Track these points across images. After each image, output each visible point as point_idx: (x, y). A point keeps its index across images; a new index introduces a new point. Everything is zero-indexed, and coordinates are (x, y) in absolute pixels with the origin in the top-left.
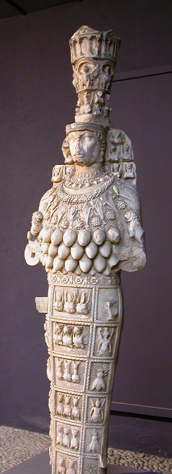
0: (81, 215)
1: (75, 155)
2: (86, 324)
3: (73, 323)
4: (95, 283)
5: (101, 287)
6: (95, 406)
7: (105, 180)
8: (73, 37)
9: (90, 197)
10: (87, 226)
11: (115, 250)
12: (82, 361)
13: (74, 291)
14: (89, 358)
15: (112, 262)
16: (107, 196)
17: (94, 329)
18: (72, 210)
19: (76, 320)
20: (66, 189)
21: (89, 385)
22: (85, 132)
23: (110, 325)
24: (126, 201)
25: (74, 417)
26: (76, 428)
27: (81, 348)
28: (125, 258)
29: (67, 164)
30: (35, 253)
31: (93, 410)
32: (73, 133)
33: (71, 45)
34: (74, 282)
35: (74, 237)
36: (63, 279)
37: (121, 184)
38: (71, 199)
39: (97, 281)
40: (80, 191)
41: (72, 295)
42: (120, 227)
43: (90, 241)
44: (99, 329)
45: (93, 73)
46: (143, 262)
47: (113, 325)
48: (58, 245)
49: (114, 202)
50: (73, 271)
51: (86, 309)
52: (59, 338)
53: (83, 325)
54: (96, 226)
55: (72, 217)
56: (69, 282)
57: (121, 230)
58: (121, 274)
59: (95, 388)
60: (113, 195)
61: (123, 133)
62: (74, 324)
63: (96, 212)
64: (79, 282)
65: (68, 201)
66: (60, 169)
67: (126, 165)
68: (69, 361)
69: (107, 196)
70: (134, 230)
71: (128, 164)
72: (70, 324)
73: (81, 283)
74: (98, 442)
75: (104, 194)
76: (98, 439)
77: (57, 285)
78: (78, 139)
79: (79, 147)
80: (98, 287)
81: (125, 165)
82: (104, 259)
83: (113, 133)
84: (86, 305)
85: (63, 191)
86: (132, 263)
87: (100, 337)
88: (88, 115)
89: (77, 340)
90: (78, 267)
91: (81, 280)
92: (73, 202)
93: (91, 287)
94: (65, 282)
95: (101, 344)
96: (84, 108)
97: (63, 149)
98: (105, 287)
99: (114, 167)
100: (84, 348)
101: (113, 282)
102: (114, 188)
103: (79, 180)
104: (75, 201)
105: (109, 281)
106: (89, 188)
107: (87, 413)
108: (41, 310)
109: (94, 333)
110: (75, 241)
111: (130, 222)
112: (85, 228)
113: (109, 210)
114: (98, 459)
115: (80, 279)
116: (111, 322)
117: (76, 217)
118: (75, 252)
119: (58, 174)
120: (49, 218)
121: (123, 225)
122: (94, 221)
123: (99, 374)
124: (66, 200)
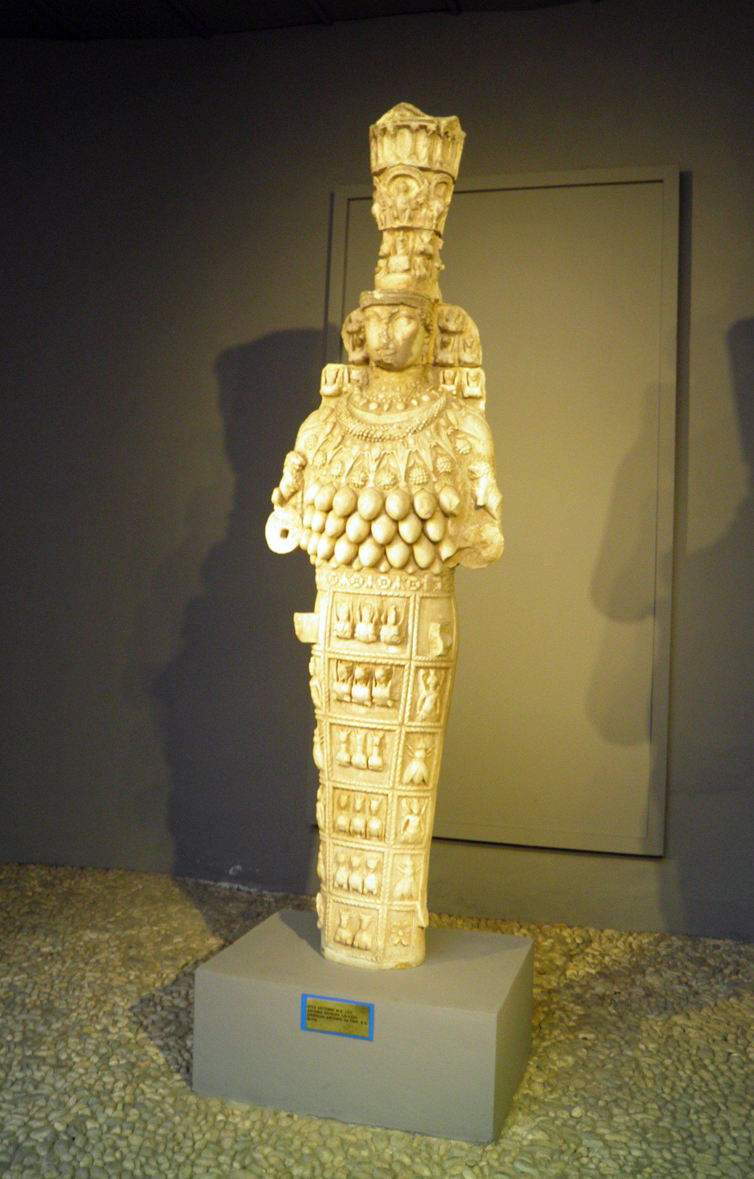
0: (392, 464)
1: (377, 350)
2: (397, 662)
3: (373, 660)
4: (414, 588)
5: (425, 595)
6: (411, 812)
7: (434, 399)
9: (407, 431)
10: (402, 484)
11: (451, 530)
12: (389, 731)
13: (375, 603)
14: (402, 724)
15: (446, 551)
16: (437, 428)
17: (412, 673)
18: (376, 451)
19: (380, 655)
20: (359, 412)
21: (402, 775)
22: (401, 307)
23: (438, 665)
24: (470, 439)
25: (371, 836)
26: (375, 855)
27: (388, 707)
28: (468, 544)
29: (353, 363)
30: (281, 532)
31: (408, 821)
32: (378, 309)
33: (375, 137)
34: (374, 586)
35: (381, 502)
36: (352, 580)
37: (461, 407)
38: (372, 432)
39: (418, 584)
40: (385, 418)
41: (372, 609)
42: (460, 488)
43: (410, 509)
44: (422, 672)
45: (416, 197)
46: (499, 552)
47: (444, 665)
48: (347, 517)
49: (451, 441)
50: (375, 566)
51: (399, 635)
52: (345, 688)
53: (392, 665)
54: (419, 484)
55: (373, 466)
57: (462, 492)
58: (457, 574)
59: (412, 781)
60: (447, 428)
61: (464, 312)
62: (375, 664)
63: (420, 457)
64: (386, 587)
65: (365, 435)
66: (337, 373)
67: (468, 374)
68: (362, 733)
69: (437, 428)
70: (486, 494)
71: (473, 372)
72: (368, 663)
73: (388, 588)
74: (415, 879)
75: (432, 427)
76: (414, 874)
77: (339, 590)
78: (386, 321)
80: (419, 594)
81: (465, 374)
82: (431, 545)
83: (445, 312)
84: (400, 629)
85: (352, 415)
86: (480, 554)
87: (422, 686)
88: (405, 277)
89: (381, 691)
90: (357, 560)
91: (389, 582)
93: (407, 595)
94: (357, 585)
95: (424, 700)
97: (344, 335)
98: (432, 595)
99: (446, 375)
100: (394, 706)
101: (446, 587)
102: (451, 416)
103: (381, 396)
105: (439, 585)
106: (403, 414)
107: (396, 827)
108: (304, 638)
109: (411, 678)
110: (382, 510)
111: (479, 478)
112: (398, 488)
113: (442, 455)
114: (413, 911)
116: (440, 659)
117: (381, 466)
118: (381, 530)
119: (335, 381)
120: (324, 465)
121: (465, 484)
122: (417, 475)
123: (420, 754)
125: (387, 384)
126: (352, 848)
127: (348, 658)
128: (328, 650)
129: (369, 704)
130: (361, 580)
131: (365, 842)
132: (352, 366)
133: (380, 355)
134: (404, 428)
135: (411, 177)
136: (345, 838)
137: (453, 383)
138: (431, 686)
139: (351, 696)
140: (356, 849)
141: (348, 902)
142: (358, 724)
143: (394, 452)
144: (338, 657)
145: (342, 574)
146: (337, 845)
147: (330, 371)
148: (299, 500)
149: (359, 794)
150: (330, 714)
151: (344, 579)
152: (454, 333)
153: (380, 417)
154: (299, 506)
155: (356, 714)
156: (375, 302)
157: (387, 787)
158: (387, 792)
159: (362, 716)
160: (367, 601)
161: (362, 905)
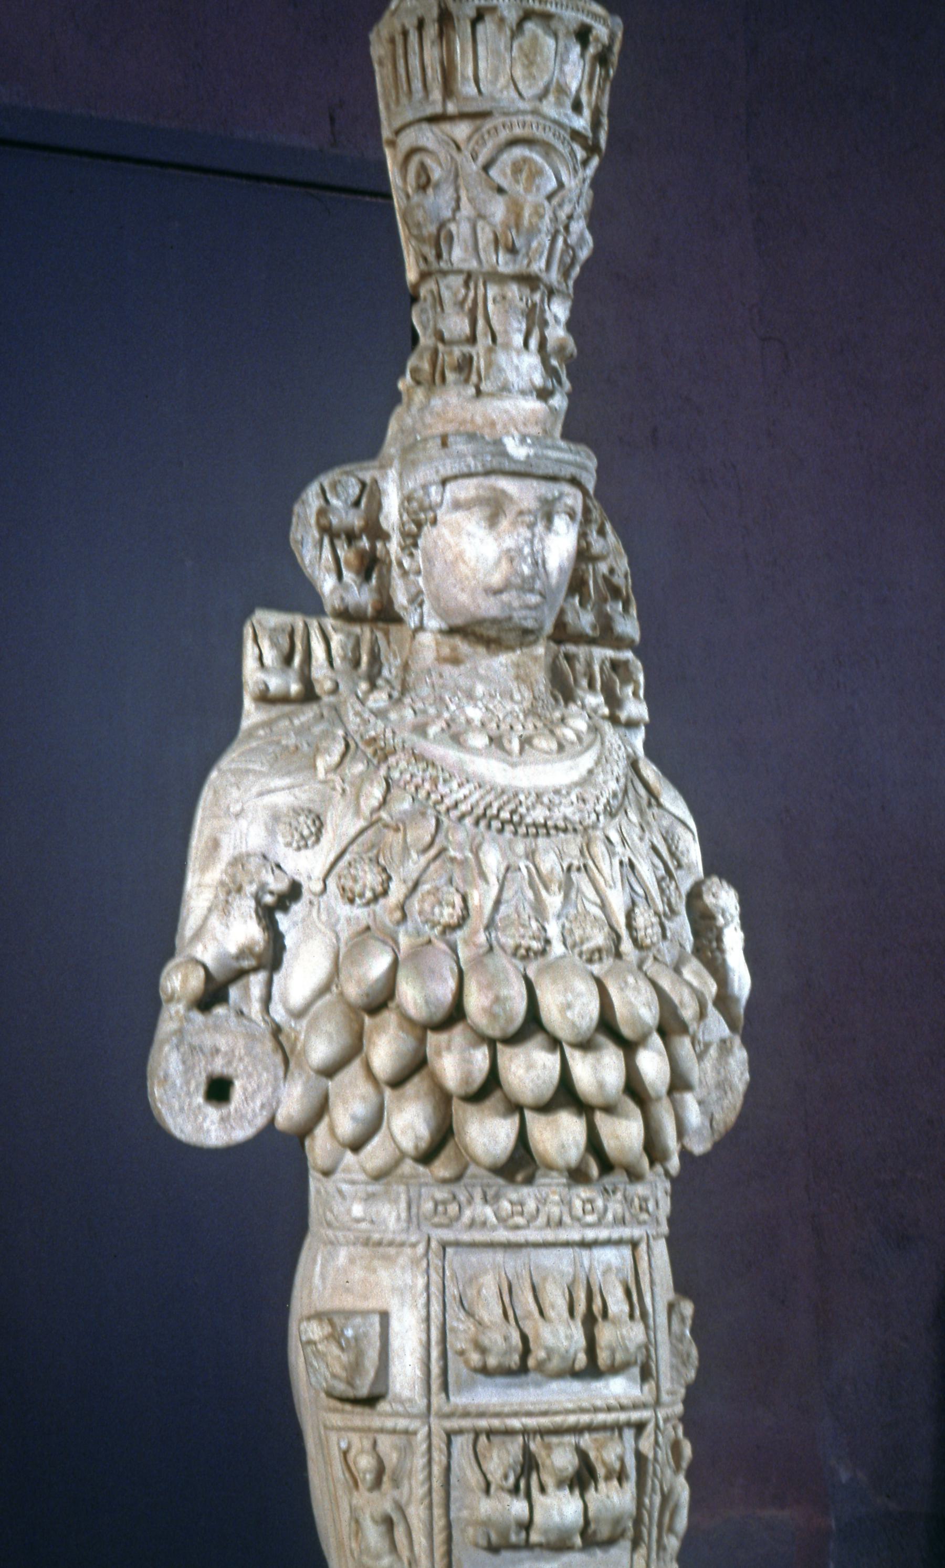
1: (497, 592)
9: (600, 808)
34: (567, 1219)
38: (522, 810)
52: (519, 1507)
56: (542, 1220)
65: (505, 815)
79: (533, 554)
88: (533, 405)
92: (529, 820)
103: (475, 713)
115: (591, 1201)
127: (516, 1423)
128: (446, 1409)
129: (578, 1541)
133: (504, 605)
134: (591, 801)
135: (547, 149)
137: (591, 686)
138: (685, 1464)
139: (527, 1526)
144: (483, 1423)
153: (519, 771)
156: (507, 465)
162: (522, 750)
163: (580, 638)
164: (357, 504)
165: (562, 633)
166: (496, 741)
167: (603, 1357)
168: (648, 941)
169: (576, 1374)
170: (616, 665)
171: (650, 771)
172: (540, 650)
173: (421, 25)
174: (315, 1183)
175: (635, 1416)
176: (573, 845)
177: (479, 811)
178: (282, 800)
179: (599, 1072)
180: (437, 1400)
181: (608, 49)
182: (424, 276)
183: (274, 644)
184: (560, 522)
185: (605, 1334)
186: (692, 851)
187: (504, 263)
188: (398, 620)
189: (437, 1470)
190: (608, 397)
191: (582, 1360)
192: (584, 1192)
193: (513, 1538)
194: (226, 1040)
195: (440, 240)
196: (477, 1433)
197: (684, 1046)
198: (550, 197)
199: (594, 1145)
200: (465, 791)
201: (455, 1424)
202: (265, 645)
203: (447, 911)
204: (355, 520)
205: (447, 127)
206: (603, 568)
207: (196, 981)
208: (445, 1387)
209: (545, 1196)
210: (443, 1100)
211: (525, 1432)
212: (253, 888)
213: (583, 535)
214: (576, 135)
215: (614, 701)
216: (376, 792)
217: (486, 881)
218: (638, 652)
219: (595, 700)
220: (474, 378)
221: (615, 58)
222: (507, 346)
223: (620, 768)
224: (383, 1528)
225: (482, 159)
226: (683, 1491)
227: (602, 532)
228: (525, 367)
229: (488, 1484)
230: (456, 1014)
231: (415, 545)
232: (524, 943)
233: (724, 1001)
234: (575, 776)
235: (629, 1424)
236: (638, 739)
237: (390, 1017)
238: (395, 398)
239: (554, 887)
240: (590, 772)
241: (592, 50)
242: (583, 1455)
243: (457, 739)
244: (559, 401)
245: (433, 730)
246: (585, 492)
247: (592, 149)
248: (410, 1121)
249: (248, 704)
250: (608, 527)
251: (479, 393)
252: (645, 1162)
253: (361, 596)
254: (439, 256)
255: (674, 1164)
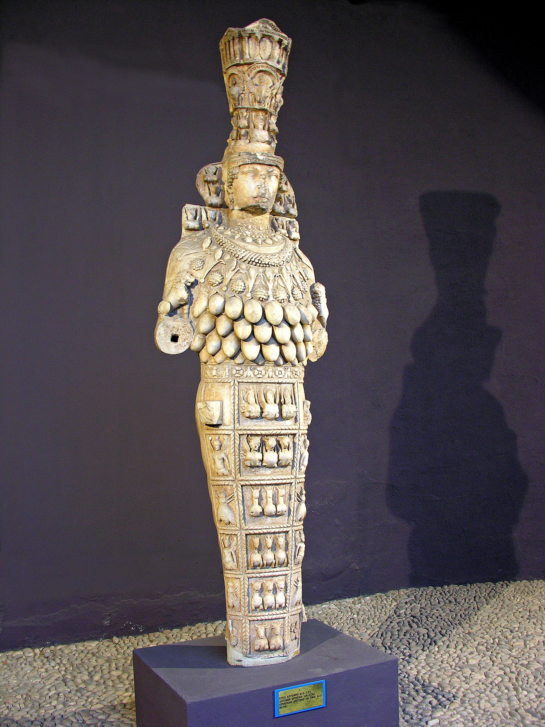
0: (281, 283)
3: (278, 432)
6: (302, 541)
8: (247, 28)
22: (275, 168)
26: (281, 577)
29: (211, 206)
32: (258, 167)
34: (274, 376)
40: (264, 250)
52: (259, 456)
65: (257, 261)
77: (244, 381)
88: (267, 146)
96: (261, 133)
104: (267, 263)
106: (275, 247)
119: (195, 218)
124: (253, 260)
125: (252, 224)
126: (265, 577)
127: (258, 432)
128: (239, 428)
129: (276, 465)
130: (263, 372)
131: (275, 569)
132: (207, 208)
133: (257, 202)
135: (270, 74)
136: (259, 570)
137: (283, 228)
138: (307, 447)
139: (262, 461)
140: (269, 577)
141: (263, 618)
142: (269, 482)
143: (281, 275)
144: (249, 432)
145: (246, 367)
146: (252, 577)
147: (189, 210)
148: (186, 311)
149: (269, 536)
150: (242, 478)
151: (249, 373)
152: (284, 191)
154: (186, 316)
155: (264, 475)
157: (289, 525)
158: (288, 529)
159: (268, 475)
160: (268, 388)
161: (274, 617)
162: (262, 243)
163: (280, 214)
164: (215, 174)
165: (274, 213)
166: (255, 241)
167: (284, 415)
168: (298, 298)
169: (276, 419)
170: (290, 222)
171: (299, 252)
172: (268, 215)
173: (233, 39)
174: (203, 367)
175: (293, 432)
176: (276, 270)
177: (249, 260)
178: (193, 257)
179: (283, 334)
180: (237, 425)
181: (287, 46)
182: (235, 109)
183: (191, 214)
184: (273, 178)
185: (285, 408)
186: (311, 274)
187: (257, 106)
188: (227, 207)
189: (237, 445)
190: (286, 143)
191: (278, 415)
192: (279, 369)
193: (258, 464)
194: (176, 324)
195: (238, 99)
196: (248, 435)
197: (308, 328)
198: (270, 88)
199: (282, 354)
200: (245, 254)
201: (241, 432)
202: (188, 213)
203: (240, 287)
204: (215, 178)
205: (241, 67)
206: (287, 194)
207: (168, 308)
208: (239, 422)
209: (268, 372)
210: (239, 341)
211: (261, 435)
212: (184, 281)
213: (280, 183)
214: (278, 70)
215: (289, 232)
216: (219, 253)
217: (251, 278)
218: (297, 219)
219: (284, 231)
220: (249, 138)
221: (289, 50)
222: (258, 128)
223: (291, 249)
224: (222, 461)
225: (251, 76)
226: (306, 454)
227: (286, 184)
228: (264, 135)
229: (251, 449)
230: (242, 316)
231: (232, 185)
232: (262, 296)
233: (320, 318)
234: (277, 251)
235: (292, 434)
236: (298, 243)
237: (223, 318)
238: (227, 145)
239: (271, 281)
240: (282, 250)
241: (283, 47)
242: (278, 442)
243: (243, 240)
244: (274, 145)
245: (237, 237)
246: (280, 170)
247: (283, 75)
248: (230, 347)
249: (184, 231)
250: (288, 183)
251: (250, 142)
252: (296, 361)
253: (215, 200)
254: (239, 104)
255: (305, 363)
